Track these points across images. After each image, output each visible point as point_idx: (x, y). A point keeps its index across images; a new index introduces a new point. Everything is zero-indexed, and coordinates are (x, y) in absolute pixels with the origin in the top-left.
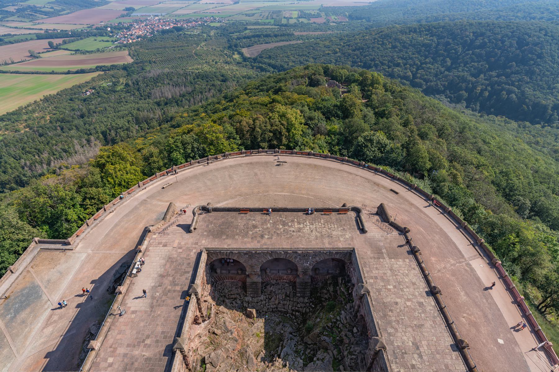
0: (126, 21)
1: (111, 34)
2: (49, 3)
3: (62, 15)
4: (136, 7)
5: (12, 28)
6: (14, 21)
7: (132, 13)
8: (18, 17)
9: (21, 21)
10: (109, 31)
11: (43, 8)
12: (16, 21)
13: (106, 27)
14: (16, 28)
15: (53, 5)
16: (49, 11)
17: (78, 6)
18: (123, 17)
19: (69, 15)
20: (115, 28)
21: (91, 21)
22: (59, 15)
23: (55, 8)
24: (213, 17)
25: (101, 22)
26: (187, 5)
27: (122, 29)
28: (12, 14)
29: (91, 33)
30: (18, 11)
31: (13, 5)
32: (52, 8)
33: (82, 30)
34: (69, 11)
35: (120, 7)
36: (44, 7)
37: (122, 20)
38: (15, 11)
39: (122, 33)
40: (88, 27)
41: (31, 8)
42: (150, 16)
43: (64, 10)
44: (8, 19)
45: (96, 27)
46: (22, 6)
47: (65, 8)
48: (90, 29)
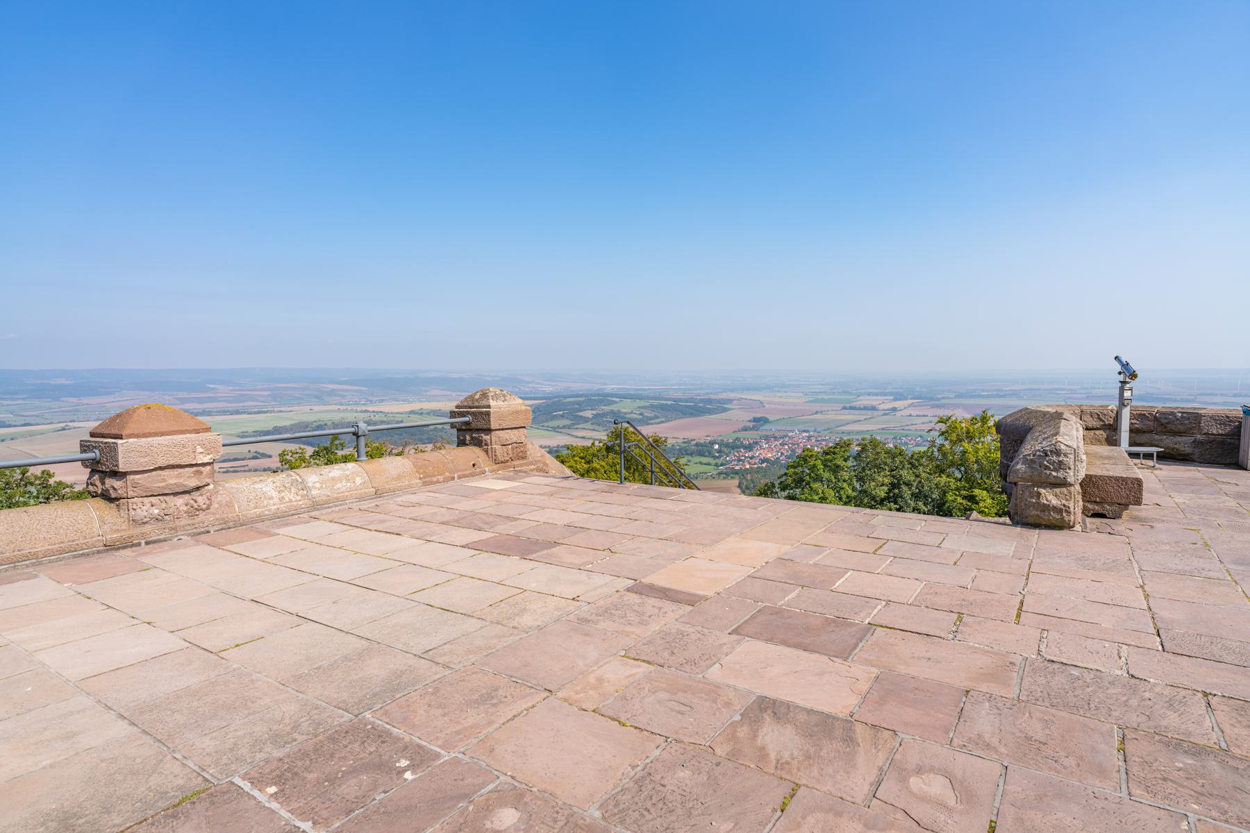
0: (748, 437)
1: (717, 454)
2: (639, 408)
3: (652, 424)
4: (771, 418)
5: (578, 437)
6: (584, 429)
7: (762, 425)
8: (592, 424)
9: (594, 430)
10: (715, 450)
11: (630, 413)
12: (588, 429)
13: (712, 443)
14: (583, 438)
15: (643, 410)
16: (637, 419)
17: (678, 413)
18: (746, 430)
19: (663, 425)
20: (727, 445)
21: (690, 435)
22: (648, 424)
23: (645, 414)
24: (921, 436)
25: (707, 436)
26: (868, 417)
27: (739, 447)
28: (586, 420)
29: (686, 451)
30: (595, 416)
31: (592, 410)
32: (641, 414)
33: (673, 445)
34: (663, 419)
35: (744, 417)
36: (632, 413)
37: (741, 435)
38: (591, 416)
39: (736, 454)
40: (685, 443)
41: (614, 413)
42: (792, 431)
43: (657, 417)
44: (577, 426)
45: (696, 443)
46: (602, 410)
47: (659, 414)
48: (687, 445)
